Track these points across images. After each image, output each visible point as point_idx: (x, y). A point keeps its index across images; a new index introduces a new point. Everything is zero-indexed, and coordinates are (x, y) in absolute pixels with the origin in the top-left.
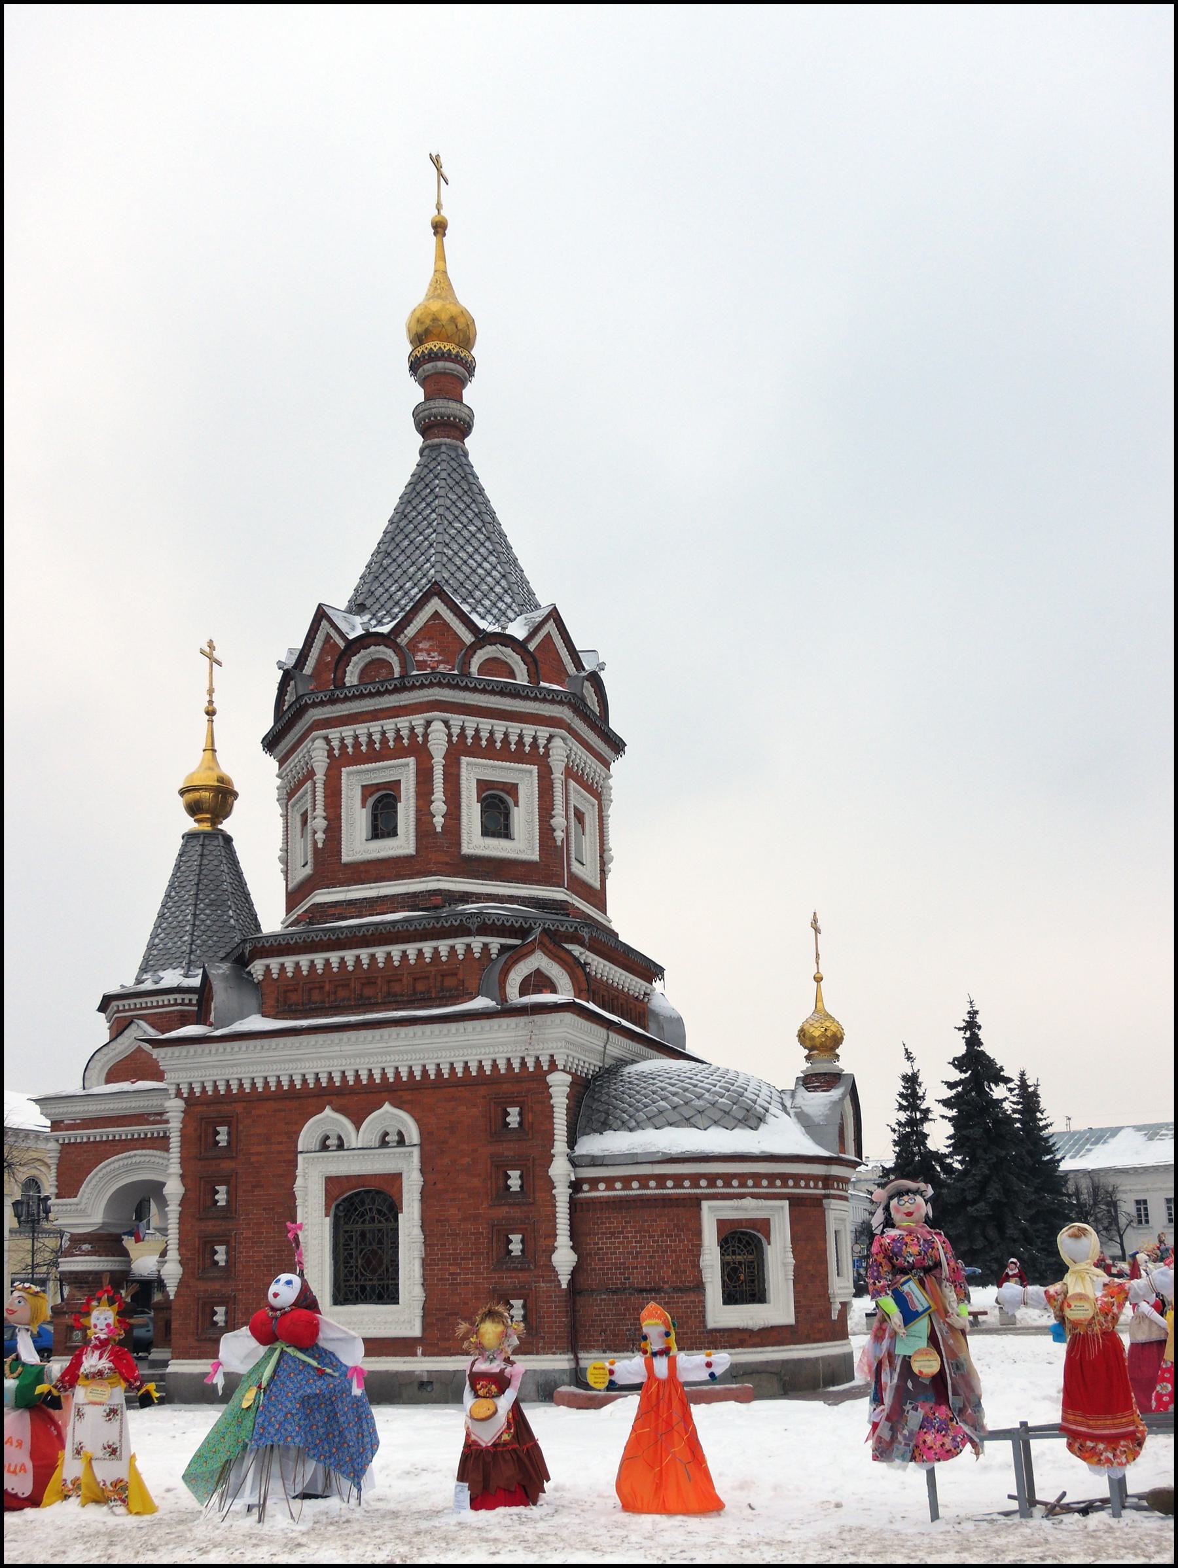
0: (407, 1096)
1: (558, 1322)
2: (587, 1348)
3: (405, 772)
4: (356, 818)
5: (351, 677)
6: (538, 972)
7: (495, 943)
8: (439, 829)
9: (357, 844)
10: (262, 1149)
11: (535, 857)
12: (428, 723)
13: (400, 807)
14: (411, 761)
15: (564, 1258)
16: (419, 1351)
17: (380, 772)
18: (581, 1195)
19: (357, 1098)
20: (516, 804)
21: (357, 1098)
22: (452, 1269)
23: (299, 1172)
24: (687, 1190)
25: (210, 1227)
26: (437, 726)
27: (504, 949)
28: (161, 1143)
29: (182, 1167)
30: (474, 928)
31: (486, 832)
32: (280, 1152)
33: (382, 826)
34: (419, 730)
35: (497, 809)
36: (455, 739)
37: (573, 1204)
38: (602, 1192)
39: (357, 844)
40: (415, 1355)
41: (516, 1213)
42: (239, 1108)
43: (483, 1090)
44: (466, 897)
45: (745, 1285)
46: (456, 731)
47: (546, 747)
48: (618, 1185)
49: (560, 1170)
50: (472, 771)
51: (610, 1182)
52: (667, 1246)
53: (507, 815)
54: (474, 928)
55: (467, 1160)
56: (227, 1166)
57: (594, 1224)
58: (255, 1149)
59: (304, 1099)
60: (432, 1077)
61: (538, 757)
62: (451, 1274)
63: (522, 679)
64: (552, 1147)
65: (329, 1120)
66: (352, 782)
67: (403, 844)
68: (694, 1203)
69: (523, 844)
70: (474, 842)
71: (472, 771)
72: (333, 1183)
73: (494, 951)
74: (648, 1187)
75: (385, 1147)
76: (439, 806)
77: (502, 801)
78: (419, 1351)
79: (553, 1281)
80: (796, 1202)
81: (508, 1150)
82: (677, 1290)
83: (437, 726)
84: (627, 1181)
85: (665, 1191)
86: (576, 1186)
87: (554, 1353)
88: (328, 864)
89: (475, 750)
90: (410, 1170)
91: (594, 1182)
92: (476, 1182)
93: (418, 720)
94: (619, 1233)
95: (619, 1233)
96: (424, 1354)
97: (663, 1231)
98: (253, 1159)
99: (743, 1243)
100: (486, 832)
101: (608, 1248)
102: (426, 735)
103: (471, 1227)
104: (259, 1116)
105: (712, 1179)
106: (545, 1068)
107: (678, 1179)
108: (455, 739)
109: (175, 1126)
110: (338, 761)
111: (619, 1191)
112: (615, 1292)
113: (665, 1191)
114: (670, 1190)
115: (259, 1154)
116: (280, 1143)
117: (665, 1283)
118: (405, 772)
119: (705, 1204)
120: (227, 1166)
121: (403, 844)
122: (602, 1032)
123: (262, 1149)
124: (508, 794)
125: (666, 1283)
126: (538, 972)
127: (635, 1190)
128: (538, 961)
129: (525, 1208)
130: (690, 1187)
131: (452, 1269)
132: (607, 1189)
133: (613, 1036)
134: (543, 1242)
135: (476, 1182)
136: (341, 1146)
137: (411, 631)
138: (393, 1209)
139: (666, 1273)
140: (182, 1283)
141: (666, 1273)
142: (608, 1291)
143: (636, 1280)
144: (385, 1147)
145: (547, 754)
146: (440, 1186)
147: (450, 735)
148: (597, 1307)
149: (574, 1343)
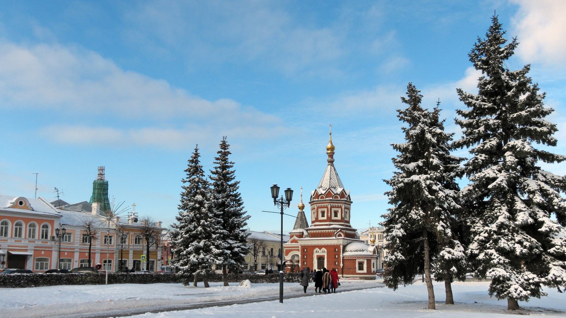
3: (326, 210)
4: (320, 215)
9: (320, 218)
15: (341, 265)
17: (323, 210)
19: (320, 247)
21: (320, 247)
28: (298, 250)
33: (323, 216)
37: (343, 259)
39: (320, 218)
45: (361, 268)
49: (341, 256)
50: (333, 209)
59: (314, 247)
63: (339, 199)
65: (317, 249)
66: (320, 210)
67: (325, 218)
69: (339, 218)
70: (334, 218)
71: (333, 209)
75: (323, 252)
80: (367, 260)
88: (317, 220)
89: (334, 207)
90: (325, 255)
99: (361, 264)
109: (300, 249)
110: (318, 208)
118: (326, 210)
121: (325, 218)
138: (324, 259)
144: (323, 252)
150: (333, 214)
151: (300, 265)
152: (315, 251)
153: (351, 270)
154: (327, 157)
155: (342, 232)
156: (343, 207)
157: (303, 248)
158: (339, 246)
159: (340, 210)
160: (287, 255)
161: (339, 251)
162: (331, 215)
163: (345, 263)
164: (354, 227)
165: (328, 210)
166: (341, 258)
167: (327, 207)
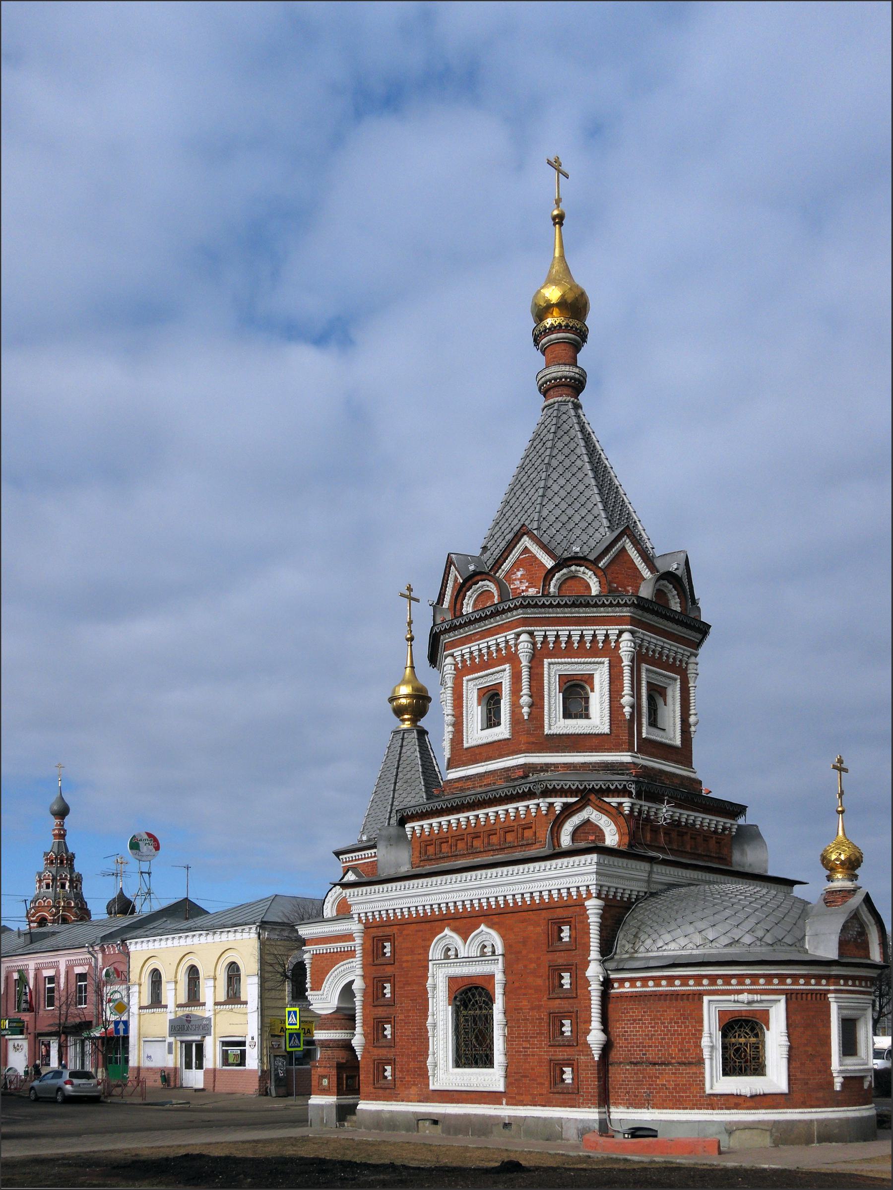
0: (496, 919)
1: (591, 1084)
2: (616, 1104)
5: (468, 607)
6: (587, 822)
7: (558, 802)
8: (526, 717)
10: (409, 958)
11: (606, 729)
12: (518, 635)
13: (502, 701)
14: (507, 666)
15: (595, 1037)
16: (504, 1102)
18: (612, 991)
19: (464, 921)
20: (592, 690)
21: (464, 921)
22: (525, 1045)
23: (430, 974)
24: (692, 986)
25: (381, 1012)
26: (524, 637)
27: (566, 806)
29: (364, 971)
30: (538, 792)
31: (567, 715)
32: (419, 960)
34: (512, 642)
35: (575, 693)
36: (539, 645)
37: (605, 997)
38: (627, 988)
40: (502, 1104)
41: (565, 1005)
42: (395, 930)
43: (544, 914)
44: (546, 767)
46: (539, 639)
47: (617, 641)
48: (638, 984)
49: (594, 971)
50: (553, 671)
51: (632, 981)
52: (675, 1031)
53: (587, 699)
54: (538, 792)
55: (533, 966)
56: (389, 970)
57: (623, 1013)
58: (405, 958)
59: (430, 923)
60: (511, 905)
61: (610, 651)
62: (524, 1048)
64: (589, 955)
68: (700, 995)
69: (598, 719)
70: (557, 723)
72: (452, 980)
73: (558, 808)
74: (660, 986)
75: (480, 955)
76: (525, 700)
77: (583, 688)
78: (504, 1102)
79: (588, 1055)
81: (561, 959)
82: (680, 1064)
83: (524, 637)
84: (644, 980)
85: (660, 989)
86: (607, 983)
87: (590, 1107)
89: (556, 652)
91: (622, 981)
92: (539, 981)
93: (510, 635)
94: (640, 1020)
95: (640, 1020)
96: (507, 1104)
97: (671, 1019)
98: (404, 965)
100: (567, 715)
101: (631, 1031)
102: (516, 645)
103: (535, 1014)
104: (407, 935)
105: (713, 979)
106: (584, 896)
107: (684, 979)
108: (539, 645)
109: (358, 941)
111: (639, 988)
112: (636, 1064)
113: (660, 989)
114: (677, 986)
115: (407, 961)
116: (419, 954)
117: (672, 1058)
119: (706, 999)
120: (389, 970)
122: (646, 866)
123: (409, 958)
124: (586, 682)
125: (674, 1058)
126: (587, 822)
127: (651, 987)
128: (590, 813)
129: (571, 1001)
130: (694, 985)
131: (525, 1045)
132: (631, 986)
133: (657, 868)
134: (582, 1026)
135: (539, 981)
136: (457, 955)
137: (506, 566)
138: (491, 1000)
139: (673, 1050)
140: (365, 1050)
141: (673, 1050)
142: (632, 1063)
143: (651, 1056)
144: (480, 955)
145: (617, 647)
146: (517, 984)
147: (534, 644)
148: (618, 1075)
149: (604, 1100)
150: (554, 701)
151: (358, 1041)
152: (435, 952)
153: (666, 1077)
154: (534, 364)
155: (615, 813)
156: (626, 646)
157: (379, 933)
158: (579, 904)
159: (601, 676)
160: (317, 987)
161: (580, 943)
162: (537, 704)
163: (617, 1029)
164: (716, 787)
165: (516, 678)
166: (595, 990)
167: (512, 658)
